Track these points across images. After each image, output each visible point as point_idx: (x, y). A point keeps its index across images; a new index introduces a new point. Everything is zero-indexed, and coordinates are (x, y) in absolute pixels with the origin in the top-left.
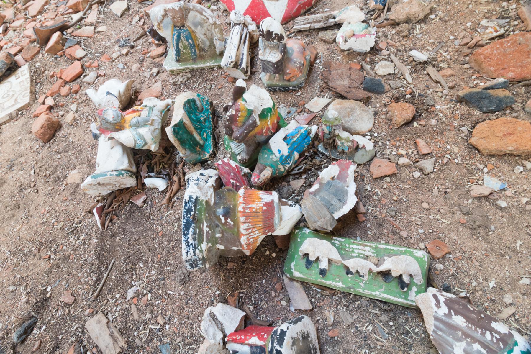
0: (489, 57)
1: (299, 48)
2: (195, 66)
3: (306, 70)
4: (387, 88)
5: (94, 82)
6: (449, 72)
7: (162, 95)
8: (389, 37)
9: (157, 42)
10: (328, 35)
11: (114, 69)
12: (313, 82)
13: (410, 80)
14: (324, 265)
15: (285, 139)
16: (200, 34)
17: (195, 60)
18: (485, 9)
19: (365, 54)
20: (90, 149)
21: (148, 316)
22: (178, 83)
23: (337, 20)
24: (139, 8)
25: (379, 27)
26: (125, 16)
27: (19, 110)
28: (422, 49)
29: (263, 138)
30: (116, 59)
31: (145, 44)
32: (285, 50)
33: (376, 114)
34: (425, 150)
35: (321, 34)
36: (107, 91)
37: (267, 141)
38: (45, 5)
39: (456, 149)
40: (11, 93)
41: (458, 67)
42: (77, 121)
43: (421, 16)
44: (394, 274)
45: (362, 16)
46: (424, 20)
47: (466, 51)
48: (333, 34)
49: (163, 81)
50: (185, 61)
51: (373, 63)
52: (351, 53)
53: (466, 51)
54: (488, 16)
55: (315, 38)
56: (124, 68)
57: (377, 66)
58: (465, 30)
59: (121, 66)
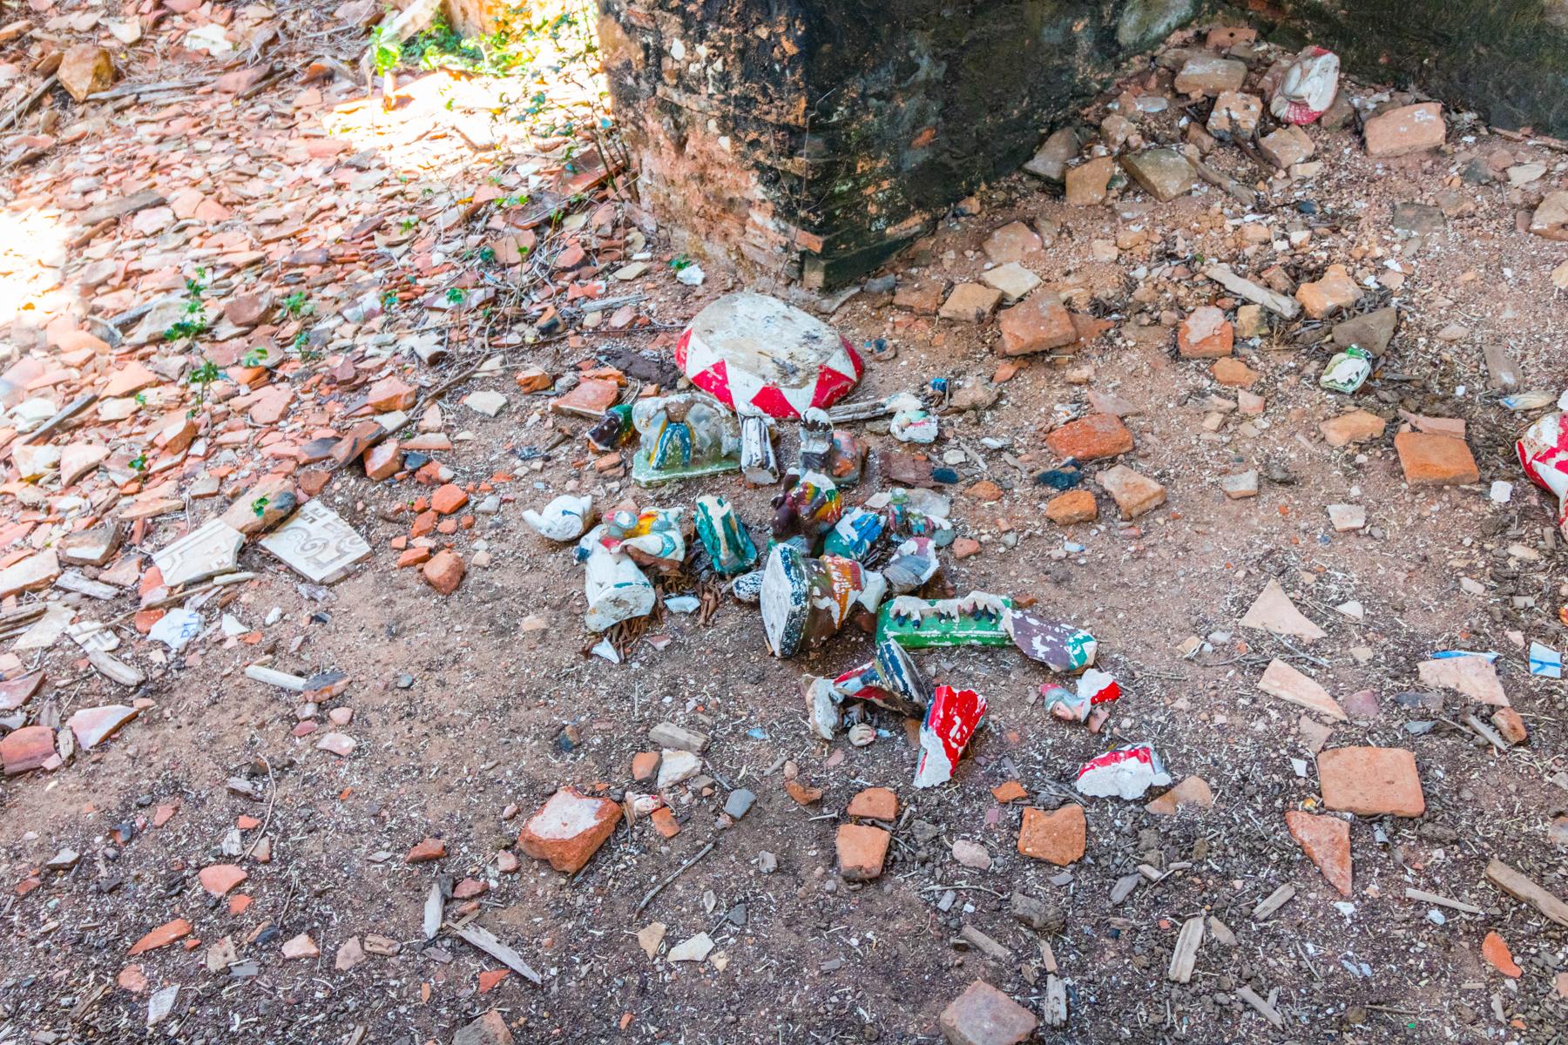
0: (1060, 439)
2: (687, 474)
3: (859, 463)
4: (960, 476)
6: (1028, 457)
9: (601, 448)
10: (879, 426)
12: (870, 479)
13: (985, 467)
14: (916, 617)
15: (853, 524)
16: (701, 432)
17: (686, 466)
18: (1058, 393)
19: (931, 445)
21: (724, 716)
25: (943, 414)
27: (356, 562)
28: (996, 436)
29: (826, 526)
32: (832, 441)
33: (952, 502)
34: (1005, 528)
35: (868, 426)
37: (832, 528)
39: (1037, 524)
40: (319, 543)
41: (1036, 452)
43: (989, 402)
44: (981, 607)
45: (918, 403)
46: (994, 406)
47: (1043, 436)
50: (672, 467)
51: (940, 453)
52: (912, 445)
53: (1043, 436)
54: (1062, 401)
59: (541, 486)
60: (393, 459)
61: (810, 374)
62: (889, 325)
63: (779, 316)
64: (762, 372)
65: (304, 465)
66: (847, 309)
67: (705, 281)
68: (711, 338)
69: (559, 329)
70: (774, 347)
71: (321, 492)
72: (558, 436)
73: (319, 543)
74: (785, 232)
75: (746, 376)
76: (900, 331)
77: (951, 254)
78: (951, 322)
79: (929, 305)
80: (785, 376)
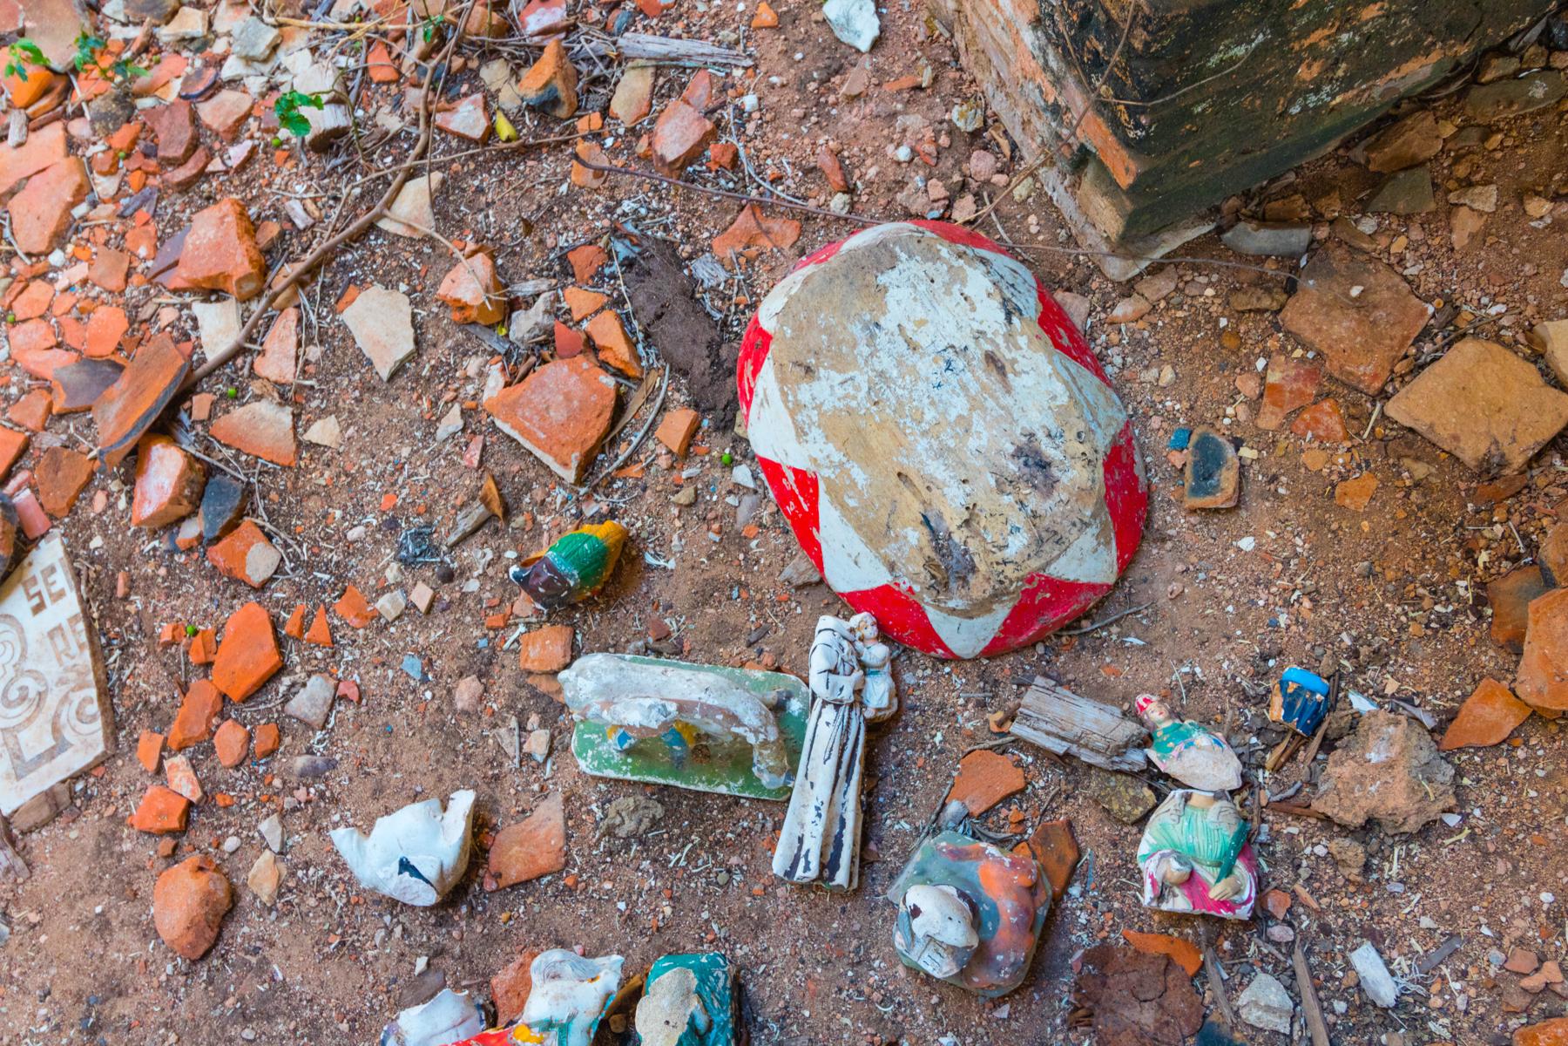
1: (1015, 914)
5: (327, 721)
7: (567, 864)
8: (1304, 873)
11: (390, 673)
17: (678, 766)
20: (344, 1027)
22: (622, 833)
23: (1152, 754)
24: (454, 348)
26: (401, 382)
27: (76, 778)
30: (392, 623)
31: (491, 572)
36: (401, 855)
38: (73, 205)
40: (33, 687)
42: (290, 897)
48: (1135, 801)
49: (567, 800)
55: (1077, 783)
56: (424, 680)
57: (1244, 997)
58: (1532, 911)
60: (175, 500)
61: (996, 596)
62: (1249, 386)
63: (977, 353)
64: (890, 550)
65: (61, 416)
66: (1164, 285)
67: (877, 44)
68: (805, 393)
69: (562, 112)
70: (937, 470)
71: (72, 510)
72: (478, 510)
73: (33, 687)
74: (1057, 81)
75: (857, 545)
76: (1269, 420)
77: (1487, 199)
78: (1411, 439)
79: (1366, 370)
80: (941, 585)
